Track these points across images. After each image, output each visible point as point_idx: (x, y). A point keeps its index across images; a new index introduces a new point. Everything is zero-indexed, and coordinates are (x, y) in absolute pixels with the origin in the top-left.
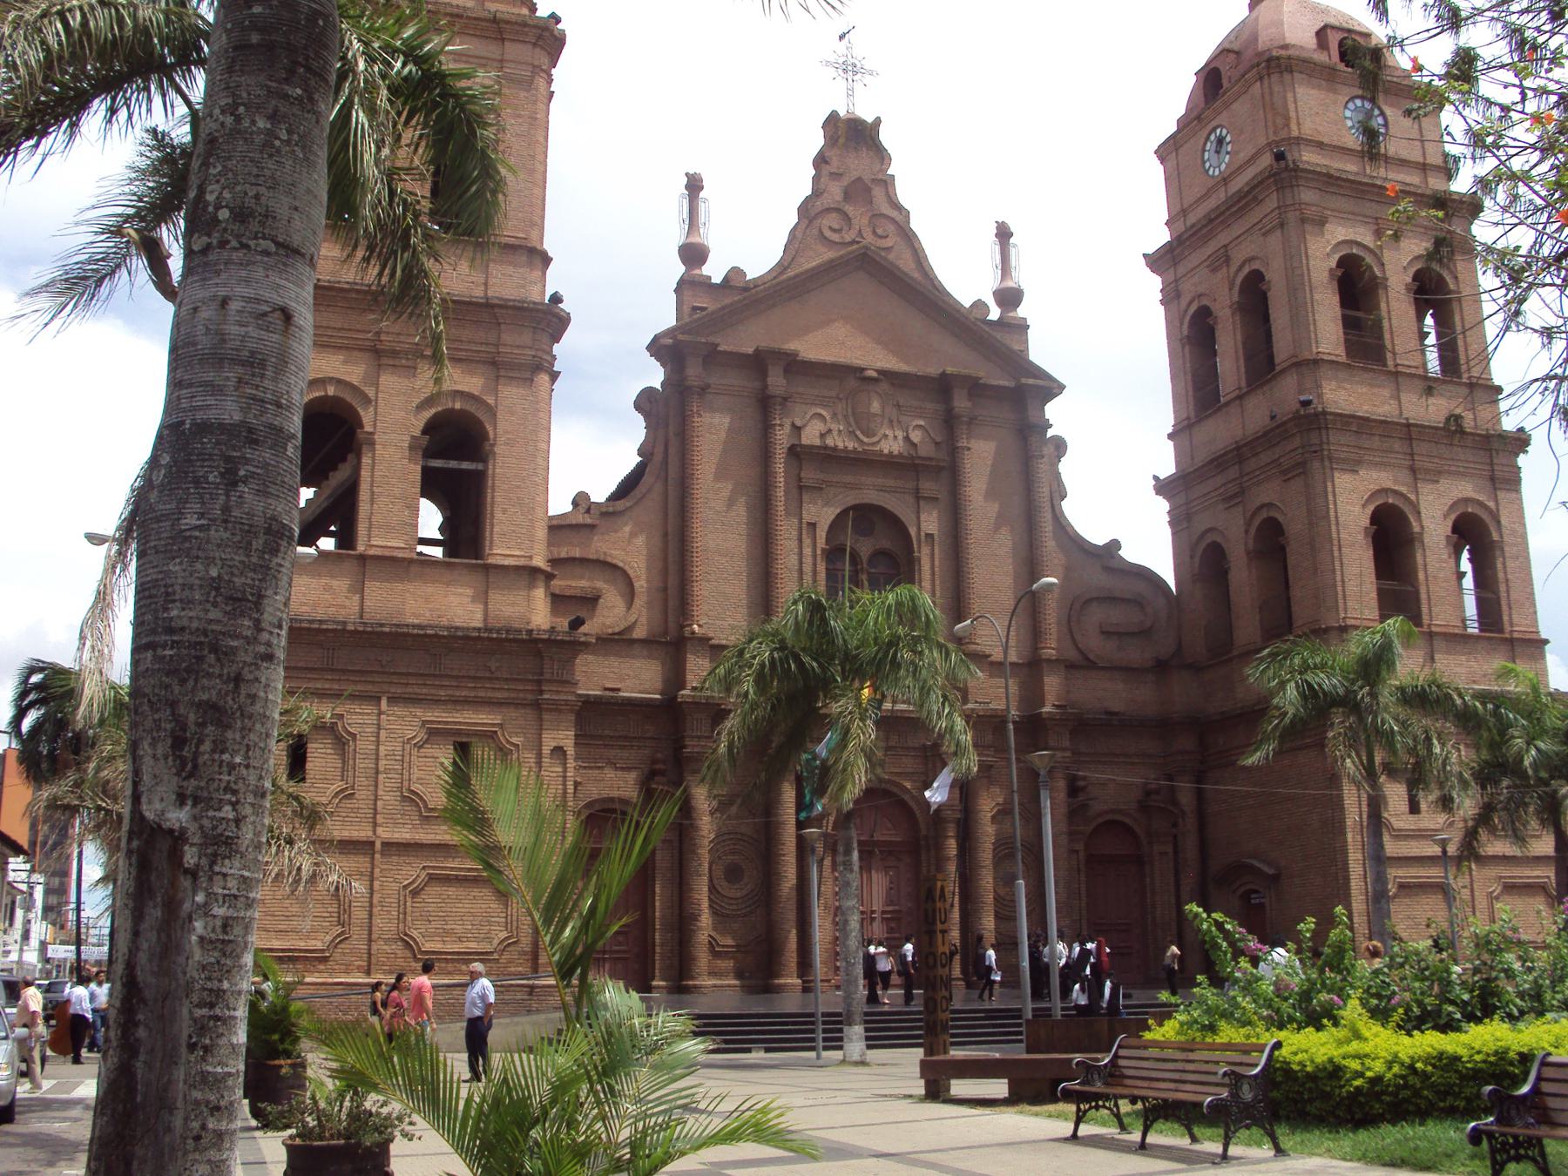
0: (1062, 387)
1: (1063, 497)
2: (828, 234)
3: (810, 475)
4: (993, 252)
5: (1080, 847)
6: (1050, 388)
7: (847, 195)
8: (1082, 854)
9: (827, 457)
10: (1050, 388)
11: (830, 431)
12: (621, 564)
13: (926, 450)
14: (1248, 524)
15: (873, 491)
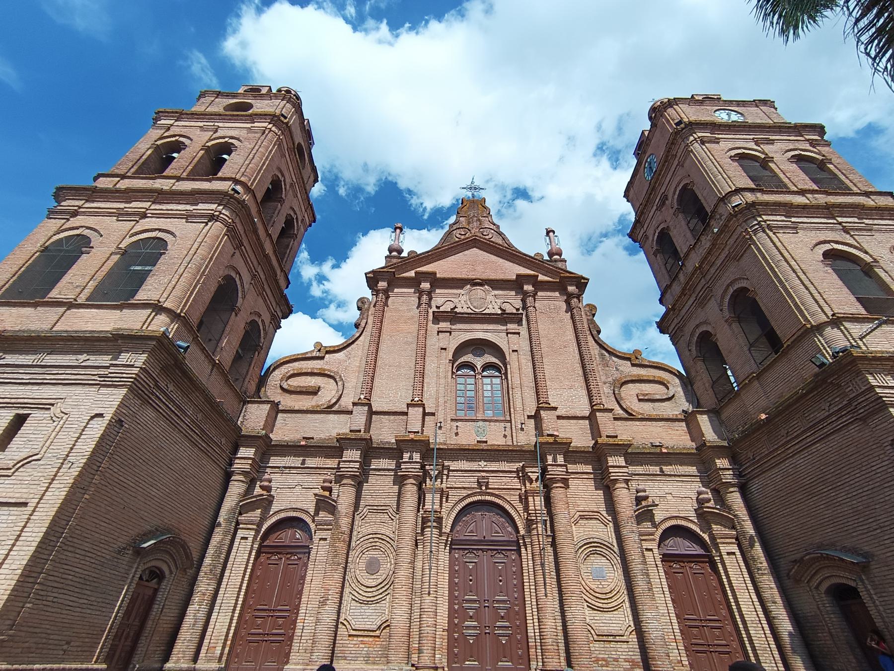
0: (588, 280)
1: (599, 332)
2: (458, 236)
3: (444, 325)
4: (545, 239)
5: (654, 545)
6: (581, 283)
7: (469, 223)
8: (656, 551)
9: (454, 317)
10: (581, 283)
11: (456, 307)
12: (332, 374)
13: (510, 309)
14: (721, 305)
15: (479, 332)
